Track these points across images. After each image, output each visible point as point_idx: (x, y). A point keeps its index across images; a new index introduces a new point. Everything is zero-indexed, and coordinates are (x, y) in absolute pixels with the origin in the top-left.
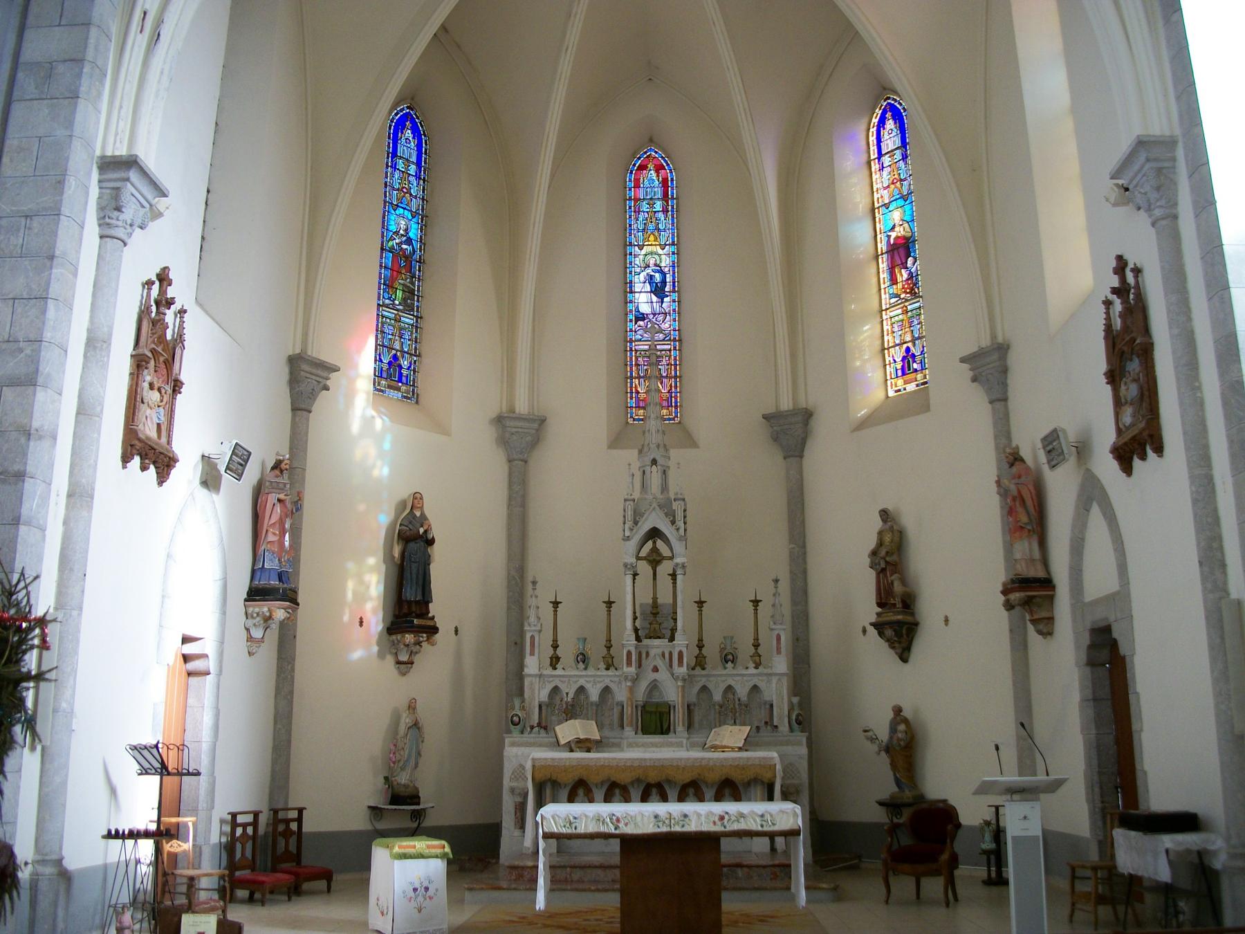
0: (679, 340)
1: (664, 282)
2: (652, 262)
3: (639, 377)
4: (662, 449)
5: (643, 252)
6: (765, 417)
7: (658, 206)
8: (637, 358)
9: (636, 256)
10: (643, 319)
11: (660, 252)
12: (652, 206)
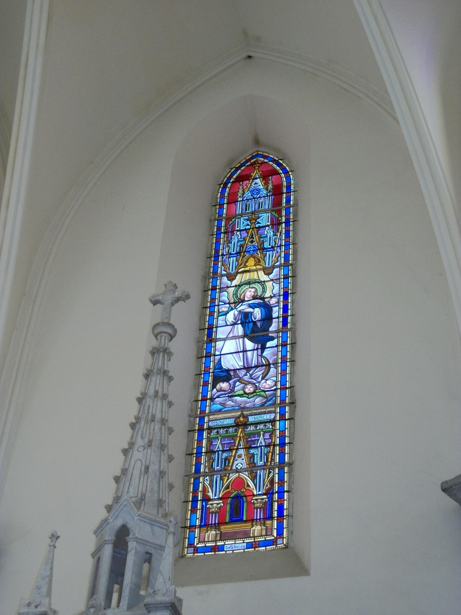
0: (285, 402)
1: (268, 318)
2: (249, 293)
3: (212, 472)
4: (149, 510)
5: (235, 282)
6: (448, 488)
7: (264, 219)
8: (210, 441)
9: (222, 290)
10: (227, 379)
11: (263, 277)
12: (253, 217)
